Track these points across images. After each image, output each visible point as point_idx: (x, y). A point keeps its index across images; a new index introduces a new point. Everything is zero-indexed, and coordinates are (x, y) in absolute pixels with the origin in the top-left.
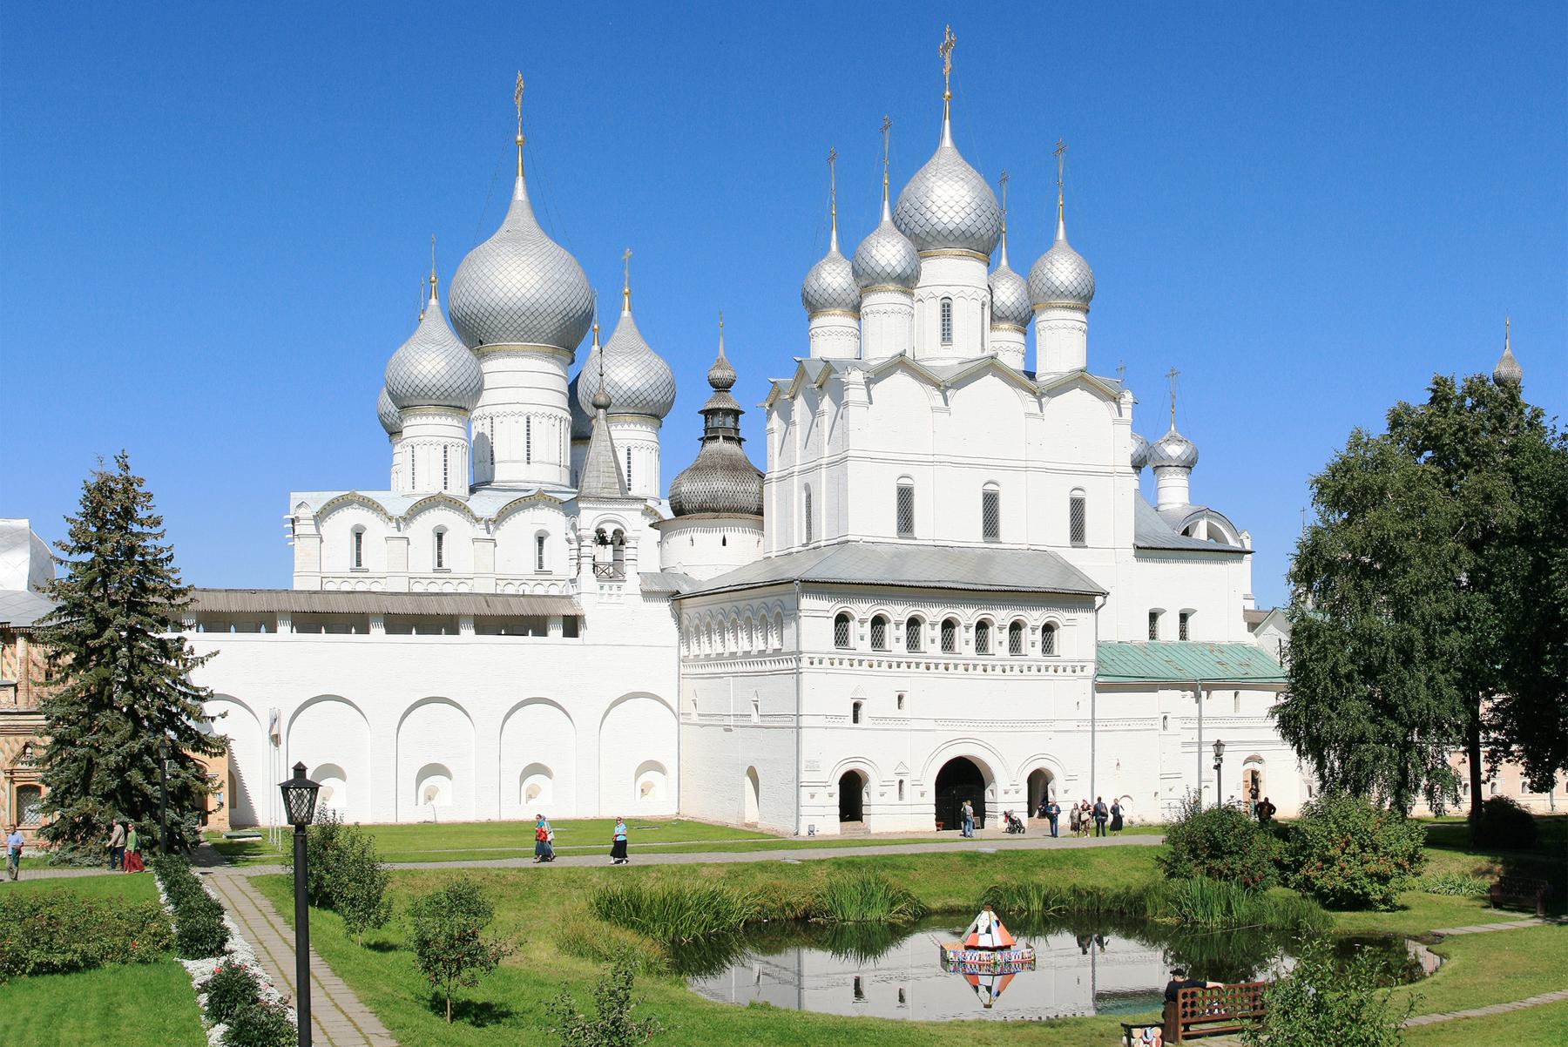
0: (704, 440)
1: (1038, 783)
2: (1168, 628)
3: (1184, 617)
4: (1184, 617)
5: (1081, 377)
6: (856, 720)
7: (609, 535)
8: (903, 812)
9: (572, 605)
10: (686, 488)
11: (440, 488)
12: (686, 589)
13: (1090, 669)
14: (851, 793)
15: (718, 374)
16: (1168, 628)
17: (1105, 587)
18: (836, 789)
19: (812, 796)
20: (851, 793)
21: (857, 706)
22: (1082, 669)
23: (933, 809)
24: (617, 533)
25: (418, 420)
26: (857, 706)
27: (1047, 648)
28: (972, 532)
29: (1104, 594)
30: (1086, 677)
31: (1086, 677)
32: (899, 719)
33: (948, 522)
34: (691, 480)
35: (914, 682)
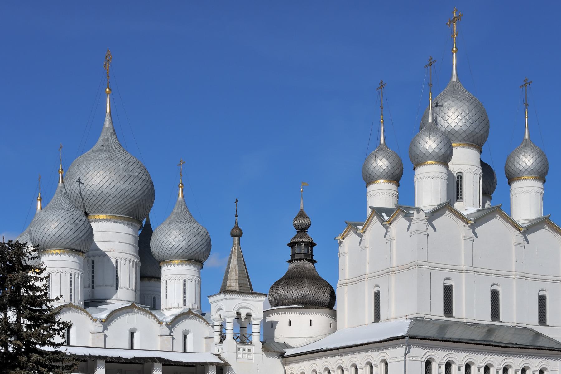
0: (290, 261)
24: (248, 315)
28: (485, 317)
33: (471, 309)
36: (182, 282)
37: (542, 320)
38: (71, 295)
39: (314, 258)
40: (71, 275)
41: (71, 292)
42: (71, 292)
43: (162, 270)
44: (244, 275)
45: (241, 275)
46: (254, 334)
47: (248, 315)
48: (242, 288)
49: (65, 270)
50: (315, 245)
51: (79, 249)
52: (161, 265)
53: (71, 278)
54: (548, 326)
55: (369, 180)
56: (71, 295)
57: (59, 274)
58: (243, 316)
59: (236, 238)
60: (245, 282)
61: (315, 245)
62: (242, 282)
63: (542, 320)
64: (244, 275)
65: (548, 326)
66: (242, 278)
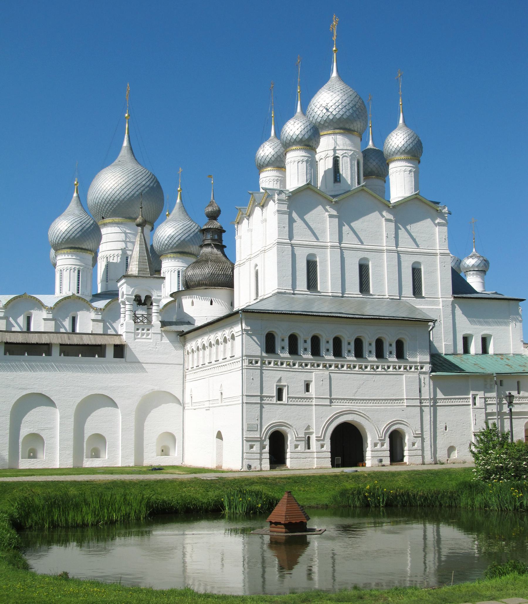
1: (396, 439)
2: (475, 347)
3: (485, 341)
4: (485, 341)
5: (416, 198)
6: (280, 397)
7: (143, 299)
8: (310, 458)
9: (121, 339)
10: (190, 273)
11: (75, 292)
12: (186, 330)
13: (427, 368)
14: (277, 444)
15: (210, 209)
16: (475, 347)
17: (433, 317)
18: (267, 443)
19: (252, 447)
20: (277, 444)
21: (280, 391)
22: (422, 368)
23: (329, 455)
25: (63, 257)
26: (280, 391)
27: (400, 355)
29: (434, 321)
30: (425, 373)
31: (425, 373)
32: (307, 398)
34: (194, 268)
35: (317, 376)
36: (176, 273)
37: (417, 291)
38: (78, 288)
39: (224, 244)
40: (79, 271)
41: (78, 285)
42: (78, 285)
43: (163, 262)
44: (144, 261)
45: (141, 261)
46: (153, 314)
47: (148, 298)
48: (141, 272)
49: (74, 266)
50: (224, 231)
51: (87, 248)
52: (161, 258)
53: (79, 273)
54: (423, 298)
55: (261, 167)
56: (78, 288)
57: (68, 271)
58: (143, 299)
59: (140, 228)
60: (145, 267)
61: (224, 231)
62: (142, 266)
63: (417, 291)
64: (144, 261)
65: (423, 298)
66: (142, 263)
